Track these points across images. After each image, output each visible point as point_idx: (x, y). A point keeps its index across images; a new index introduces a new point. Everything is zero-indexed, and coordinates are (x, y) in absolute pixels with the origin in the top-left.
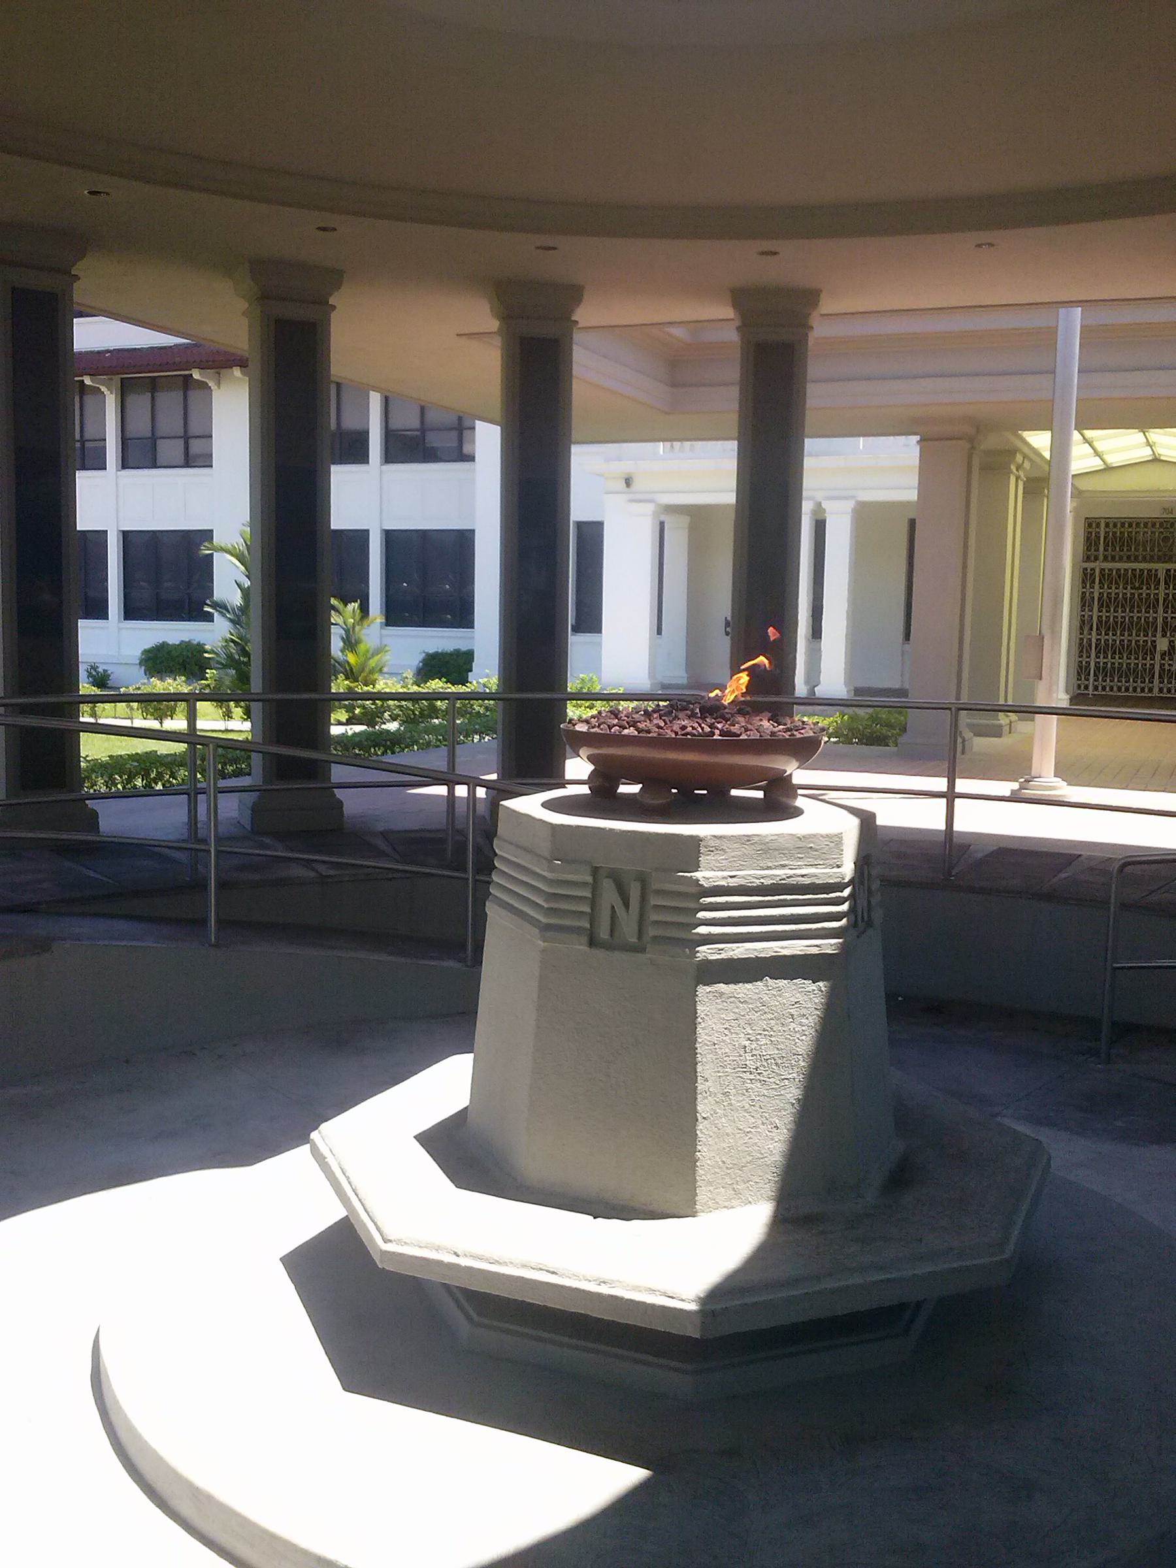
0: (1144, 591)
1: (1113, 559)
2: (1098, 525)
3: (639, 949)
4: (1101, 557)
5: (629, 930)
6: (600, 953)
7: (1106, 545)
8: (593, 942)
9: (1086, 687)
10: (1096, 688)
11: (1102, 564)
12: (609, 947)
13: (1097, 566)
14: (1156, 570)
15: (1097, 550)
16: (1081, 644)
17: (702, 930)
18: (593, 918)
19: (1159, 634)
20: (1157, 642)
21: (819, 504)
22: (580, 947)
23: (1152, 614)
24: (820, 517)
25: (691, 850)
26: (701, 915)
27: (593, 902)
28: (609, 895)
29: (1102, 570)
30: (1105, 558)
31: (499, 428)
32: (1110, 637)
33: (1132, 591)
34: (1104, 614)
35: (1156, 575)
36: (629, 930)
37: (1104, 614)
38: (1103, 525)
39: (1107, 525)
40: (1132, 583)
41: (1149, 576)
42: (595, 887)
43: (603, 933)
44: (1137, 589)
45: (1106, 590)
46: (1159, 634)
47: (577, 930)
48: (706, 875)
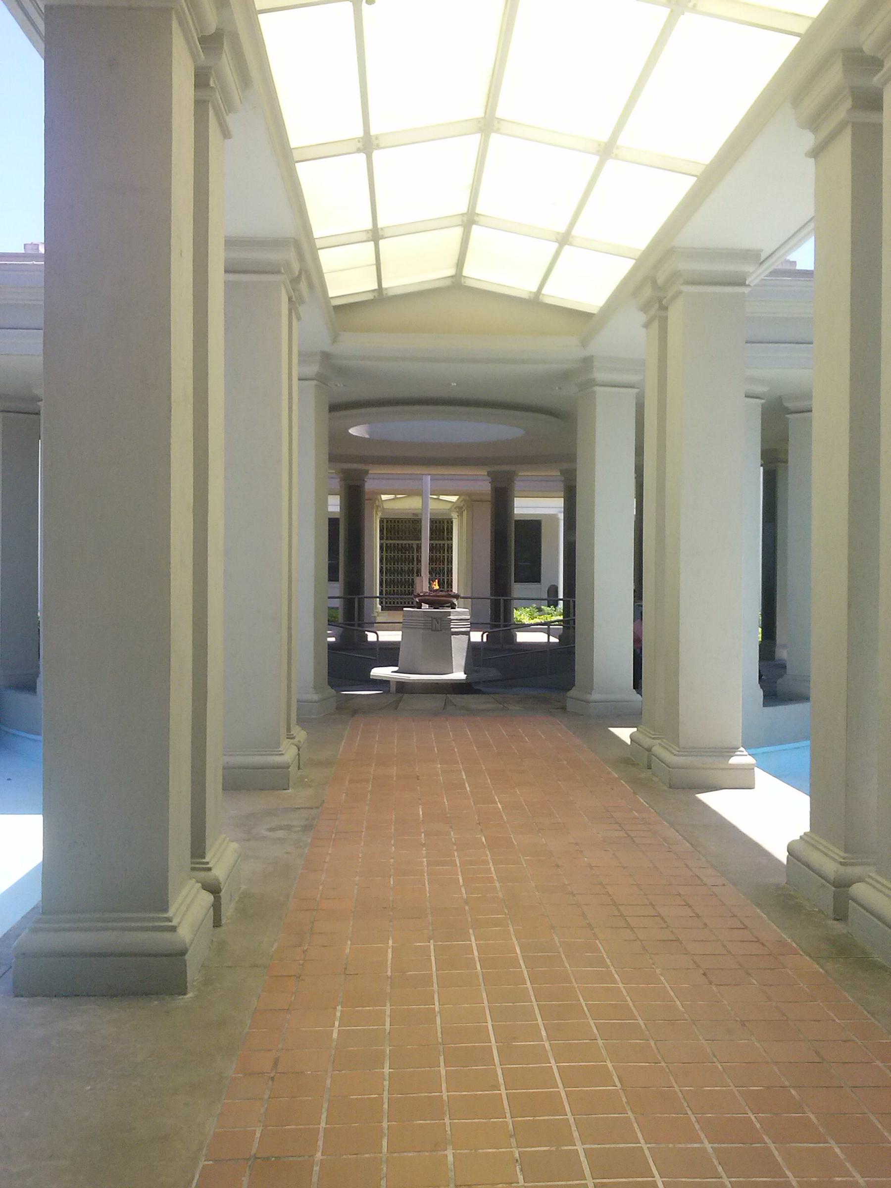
2: (383, 522)
3: (441, 630)
4: (385, 538)
8: (432, 630)
10: (386, 603)
13: (384, 542)
17: (452, 626)
22: (430, 631)
23: (411, 566)
25: (449, 614)
26: (451, 624)
28: (435, 622)
29: (386, 544)
30: (387, 539)
32: (392, 577)
33: (402, 554)
35: (412, 547)
38: (385, 522)
39: (387, 522)
40: (401, 550)
42: (432, 621)
43: (434, 628)
44: (404, 553)
45: (411, 555)
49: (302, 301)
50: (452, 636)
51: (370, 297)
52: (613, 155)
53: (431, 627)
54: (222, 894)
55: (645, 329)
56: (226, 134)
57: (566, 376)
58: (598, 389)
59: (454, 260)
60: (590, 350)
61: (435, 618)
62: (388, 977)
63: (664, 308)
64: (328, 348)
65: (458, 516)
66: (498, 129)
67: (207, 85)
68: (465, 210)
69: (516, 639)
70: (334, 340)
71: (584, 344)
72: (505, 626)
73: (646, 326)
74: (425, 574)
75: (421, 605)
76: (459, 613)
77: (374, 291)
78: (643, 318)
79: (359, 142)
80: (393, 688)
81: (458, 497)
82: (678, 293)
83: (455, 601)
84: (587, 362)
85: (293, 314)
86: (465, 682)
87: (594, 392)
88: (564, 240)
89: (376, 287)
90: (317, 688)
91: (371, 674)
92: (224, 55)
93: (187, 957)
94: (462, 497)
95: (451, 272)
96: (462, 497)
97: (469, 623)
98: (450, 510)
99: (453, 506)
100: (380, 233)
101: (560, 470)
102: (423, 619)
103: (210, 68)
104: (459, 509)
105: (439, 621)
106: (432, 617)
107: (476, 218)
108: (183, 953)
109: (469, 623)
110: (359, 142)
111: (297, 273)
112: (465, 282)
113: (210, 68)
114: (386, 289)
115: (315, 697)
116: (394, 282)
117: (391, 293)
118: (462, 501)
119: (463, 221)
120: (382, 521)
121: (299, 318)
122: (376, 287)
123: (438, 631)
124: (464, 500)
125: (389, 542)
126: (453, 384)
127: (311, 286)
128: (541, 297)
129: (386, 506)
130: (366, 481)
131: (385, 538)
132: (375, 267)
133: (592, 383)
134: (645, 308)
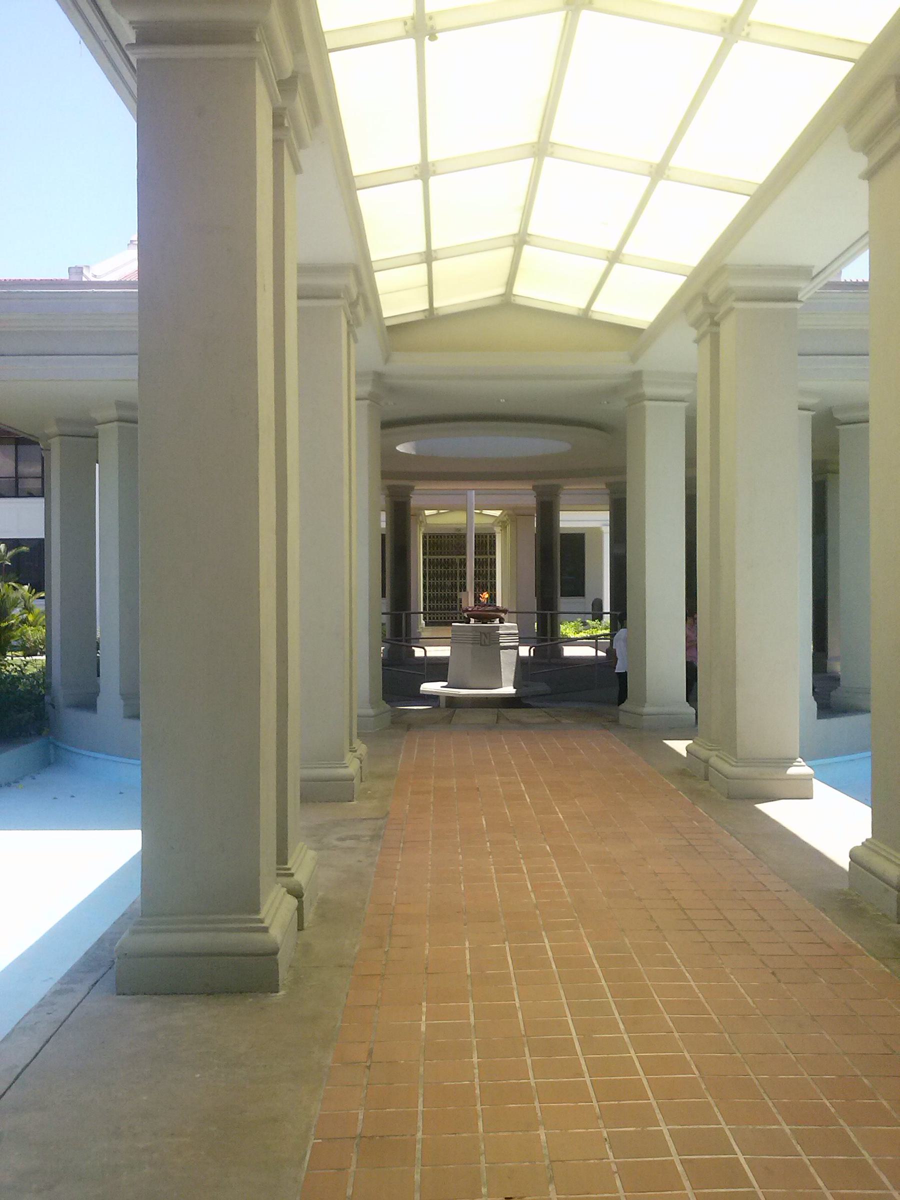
0: (450, 569)
1: (434, 554)
3: (490, 645)
4: (428, 553)
5: (487, 641)
11: (429, 557)
12: (483, 645)
13: (427, 557)
14: (455, 559)
17: (500, 641)
18: (480, 640)
19: (458, 590)
20: (458, 595)
22: (479, 646)
23: (454, 581)
25: (498, 628)
26: (500, 638)
27: (481, 638)
28: (483, 636)
29: (430, 560)
32: (435, 593)
34: (432, 581)
36: (487, 641)
37: (432, 581)
39: (430, 537)
41: (452, 562)
42: (481, 635)
43: (483, 643)
46: (458, 590)
47: (478, 643)
48: (500, 632)
49: (359, 324)
50: (501, 651)
51: (421, 317)
52: (665, 176)
54: (304, 898)
55: (696, 344)
56: (297, 169)
57: (614, 391)
58: (647, 403)
59: (504, 279)
60: (642, 364)
61: (484, 634)
62: (468, 976)
63: (717, 324)
64: (381, 367)
65: (501, 530)
66: (552, 153)
67: (282, 125)
68: (516, 231)
69: (563, 654)
70: (387, 360)
71: (634, 358)
72: (552, 640)
73: (697, 341)
74: (471, 591)
75: (470, 620)
76: (507, 628)
77: (424, 311)
78: (693, 333)
79: (416, 168)
80: (443, 703)
81: (501, 511)
82: (731, 309)
83: (503, 615)
84: (637, 377)
85: (351, 336)
86: (514, 696)
87: (644, 407)
88: (614, 258)
89: (427, 306)
90: (373, 703)
91: (421, 689)
92: (298, 98)
93: (279, 956)
94: (506, 512)
95: (501, 290)
96: (506, 512)
97: (518, 638)
98: (493, 524)
99: (496, 520)
100: (434, 255)
102: (471, 634)
103: (285, 109)
104: (503, 524)
105: (488, 635)
107: (528, 239)
108: (275, 952)
109: (518, 638)
110: (416, 168)
111: (355, 297)
112: (514, 300)
113: (285, 109)
114: (437, 309)
115: (371, 712)
116: (445, 302)
117: (441, 312)
118: (505, 515)
119: (514, 241)
120: (424, 537)
121: (356, 341)
122: (427, 306)
123: (487, 645)
126: (501, 400)
127: (367, 310)
128: (590, 313)
129: (429, 521)
130: (411, 497)
131: (428, 553)
132: (426, 288)
133: (642, 398)
134: (696, 324)
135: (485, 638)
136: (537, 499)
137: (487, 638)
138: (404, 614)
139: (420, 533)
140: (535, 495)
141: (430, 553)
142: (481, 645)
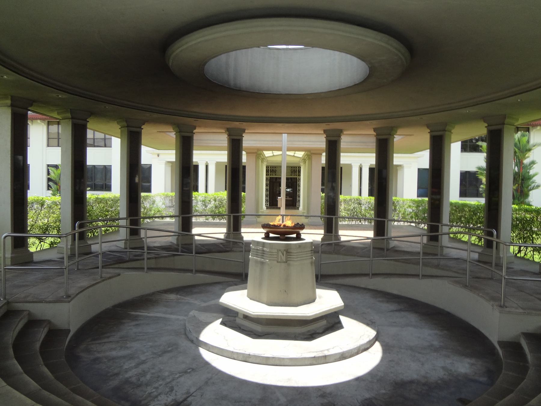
2: (269, 167)
4: (269, 175)
6: (279, 264)
7: (270, 172)
9: (267, 205)
13: (269, 176)
15: (269, 173)
16: (266, 195)
21: (207, 162)
24: (207, 164)
29: (270, 177)
31: (120, 139)
38: (270, 167)
39: (271, 167)
42: (278, 253)
53: (276, 259)
61: (280, 250)
81: (304, 152)
96: (306, 152)
101: (374, 129)
104: (304, 160)
106: (277, 250)
118: (305, 155)
124: (307, 155)
125: (270, 176)
129: (268, 159)
130: (244, 136)
131: (269, 175)
135: (282, 255)
136: (326, 139)
137: (283, 255)
138: (232, 216)
139: (262, 165)
140: (326, 136)
141: (270, 175)
142: (277, 262)
